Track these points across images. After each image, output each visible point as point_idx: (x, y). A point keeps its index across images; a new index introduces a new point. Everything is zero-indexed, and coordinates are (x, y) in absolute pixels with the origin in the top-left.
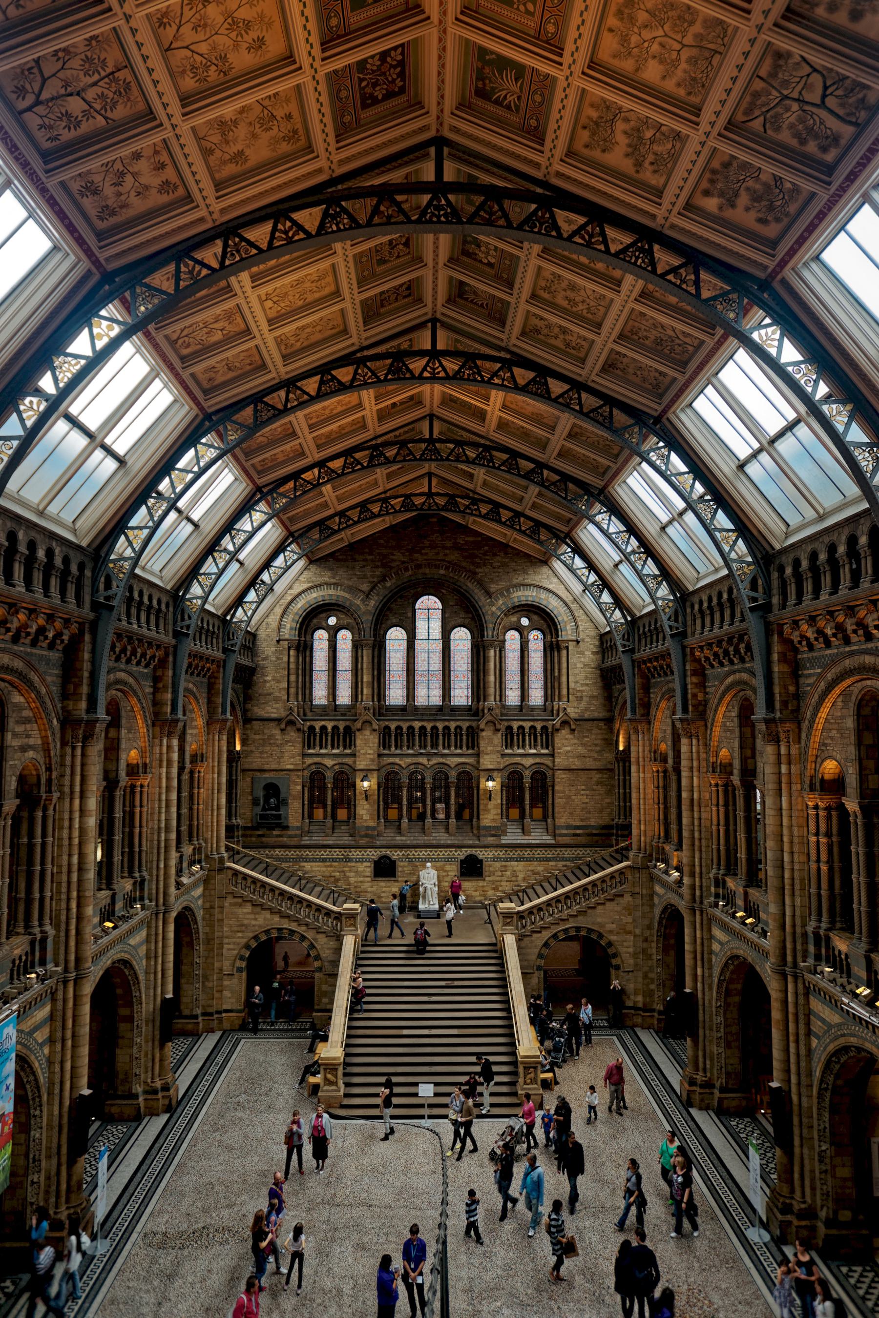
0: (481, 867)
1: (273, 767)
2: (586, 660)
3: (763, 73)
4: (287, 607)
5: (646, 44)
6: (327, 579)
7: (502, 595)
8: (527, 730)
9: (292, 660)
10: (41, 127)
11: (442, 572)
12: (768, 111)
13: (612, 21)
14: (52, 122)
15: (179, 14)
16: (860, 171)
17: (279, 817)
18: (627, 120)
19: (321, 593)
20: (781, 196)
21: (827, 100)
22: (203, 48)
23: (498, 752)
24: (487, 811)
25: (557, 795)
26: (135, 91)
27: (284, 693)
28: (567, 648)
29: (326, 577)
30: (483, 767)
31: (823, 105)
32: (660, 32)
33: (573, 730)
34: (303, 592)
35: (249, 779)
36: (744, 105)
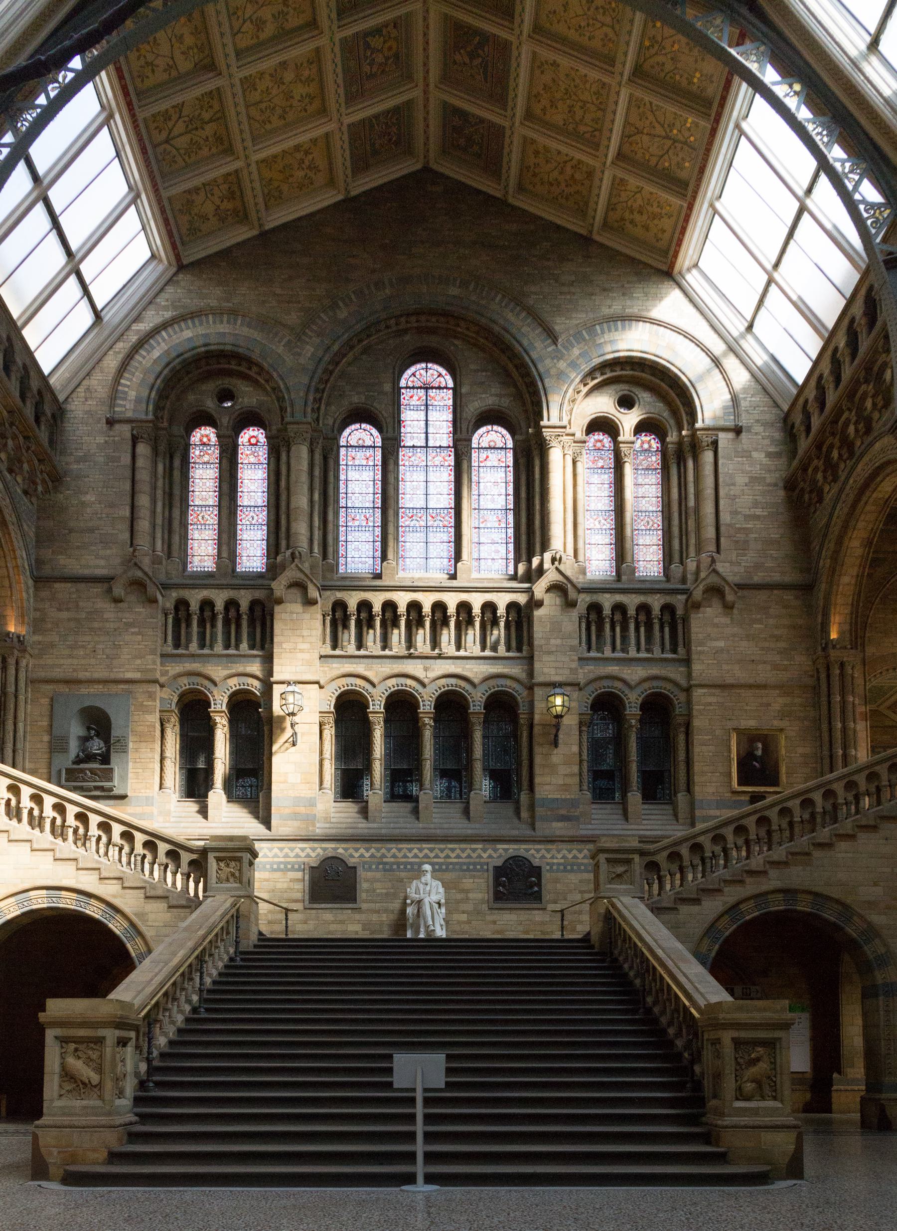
0: (539, 884)
1: (96, 676)
2: (756, 470)
4: (130, 357)
6: (214, 303)
7: (578, 337)
8: (632, 612)
9: (140, 463)
11: (454, 291)
17: (108, 775)
19: (201, 330)
23: (572, 649)
24: (552, 769)
25: (697, 738)
27: (126, 526)
28: (715, 443)
29: (214, 296)
30: (539, 678)
33: (728, 607)
34: (165, 326)
35: (45, 701)
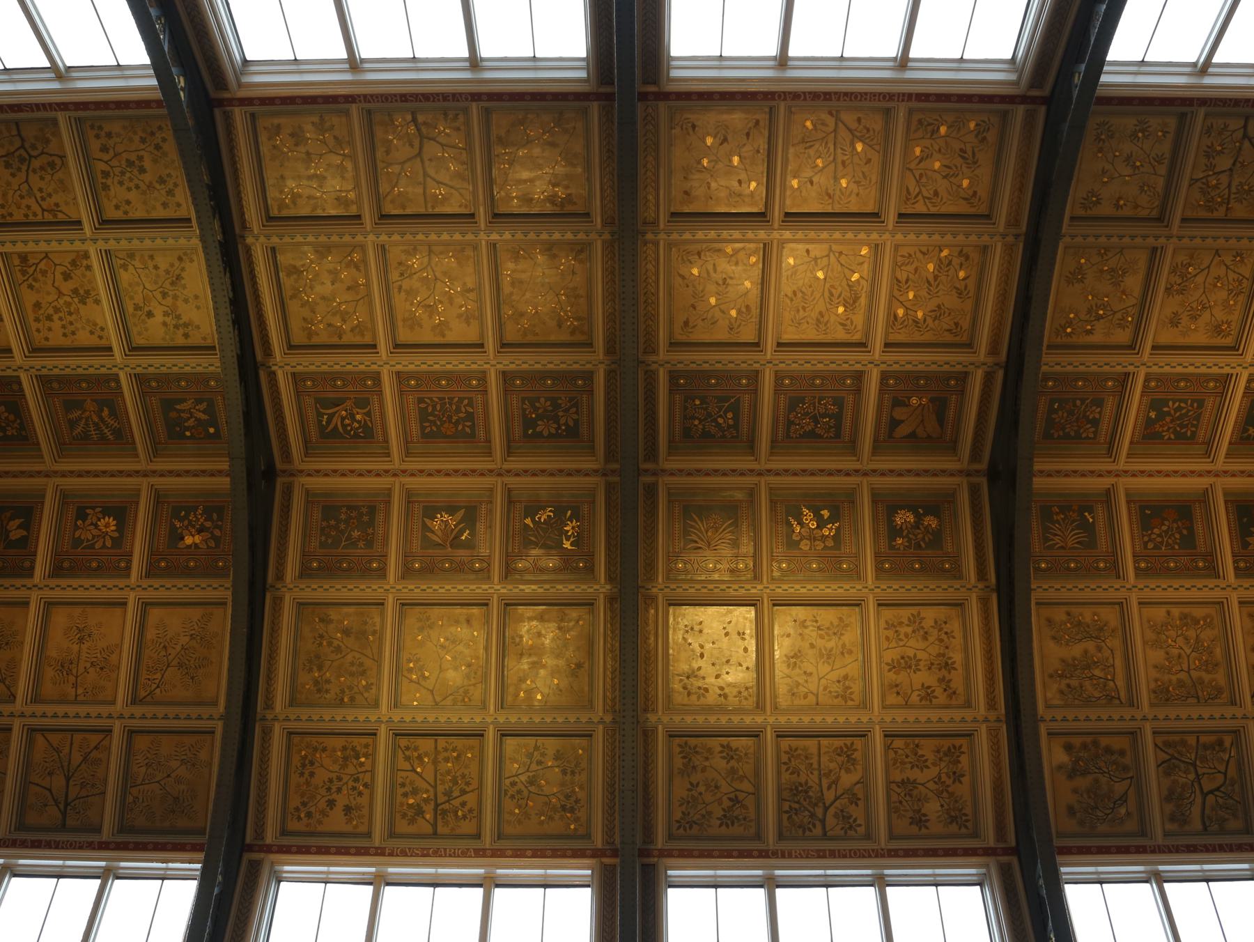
3: (1203, 739)
5: (1173, 644)
10: (1226, 126)
12: (1177, 759)
13: (1176, 611)
14: (1223, 137)
15: (1236, 270)
16: (1202, 851)
18: (1099, 649)
20: (1108, 812)
21: (1211, 795)
22: (1200, 279)
26: (1203, 214)
31: (1205, 795)
32: (1188, 651)
36: (1172, 738)
